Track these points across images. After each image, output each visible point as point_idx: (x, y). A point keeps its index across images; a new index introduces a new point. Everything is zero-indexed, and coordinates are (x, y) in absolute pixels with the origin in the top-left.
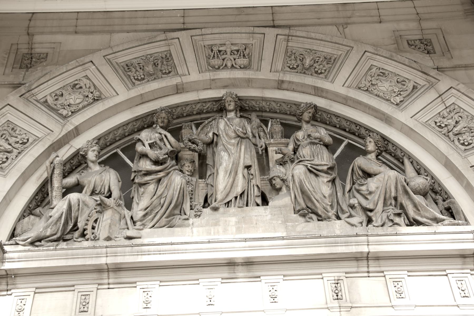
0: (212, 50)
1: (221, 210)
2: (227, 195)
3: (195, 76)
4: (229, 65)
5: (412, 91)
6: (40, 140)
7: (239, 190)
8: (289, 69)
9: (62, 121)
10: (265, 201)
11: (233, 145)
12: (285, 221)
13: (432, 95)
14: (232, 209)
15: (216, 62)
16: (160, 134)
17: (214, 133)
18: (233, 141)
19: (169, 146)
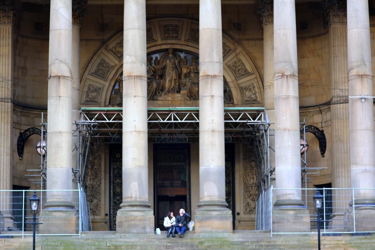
0: (165, 29)
1: (167, 94)
2: (169, 89)
3: (160, 42)
4: (171, 36)
5: (229, 51)
6: (114, 67)
7: (172, 86)
8: (191, 38)
9: (118, 59)
10: (179, 92)
11: (171, 70)
12: (185, 99)
13: (233, 55)
14: (170, 94)
15: (167, 35)
16: (149, 67)
17: (165, 64)
18: (171, 69)
19: (152, 72)
